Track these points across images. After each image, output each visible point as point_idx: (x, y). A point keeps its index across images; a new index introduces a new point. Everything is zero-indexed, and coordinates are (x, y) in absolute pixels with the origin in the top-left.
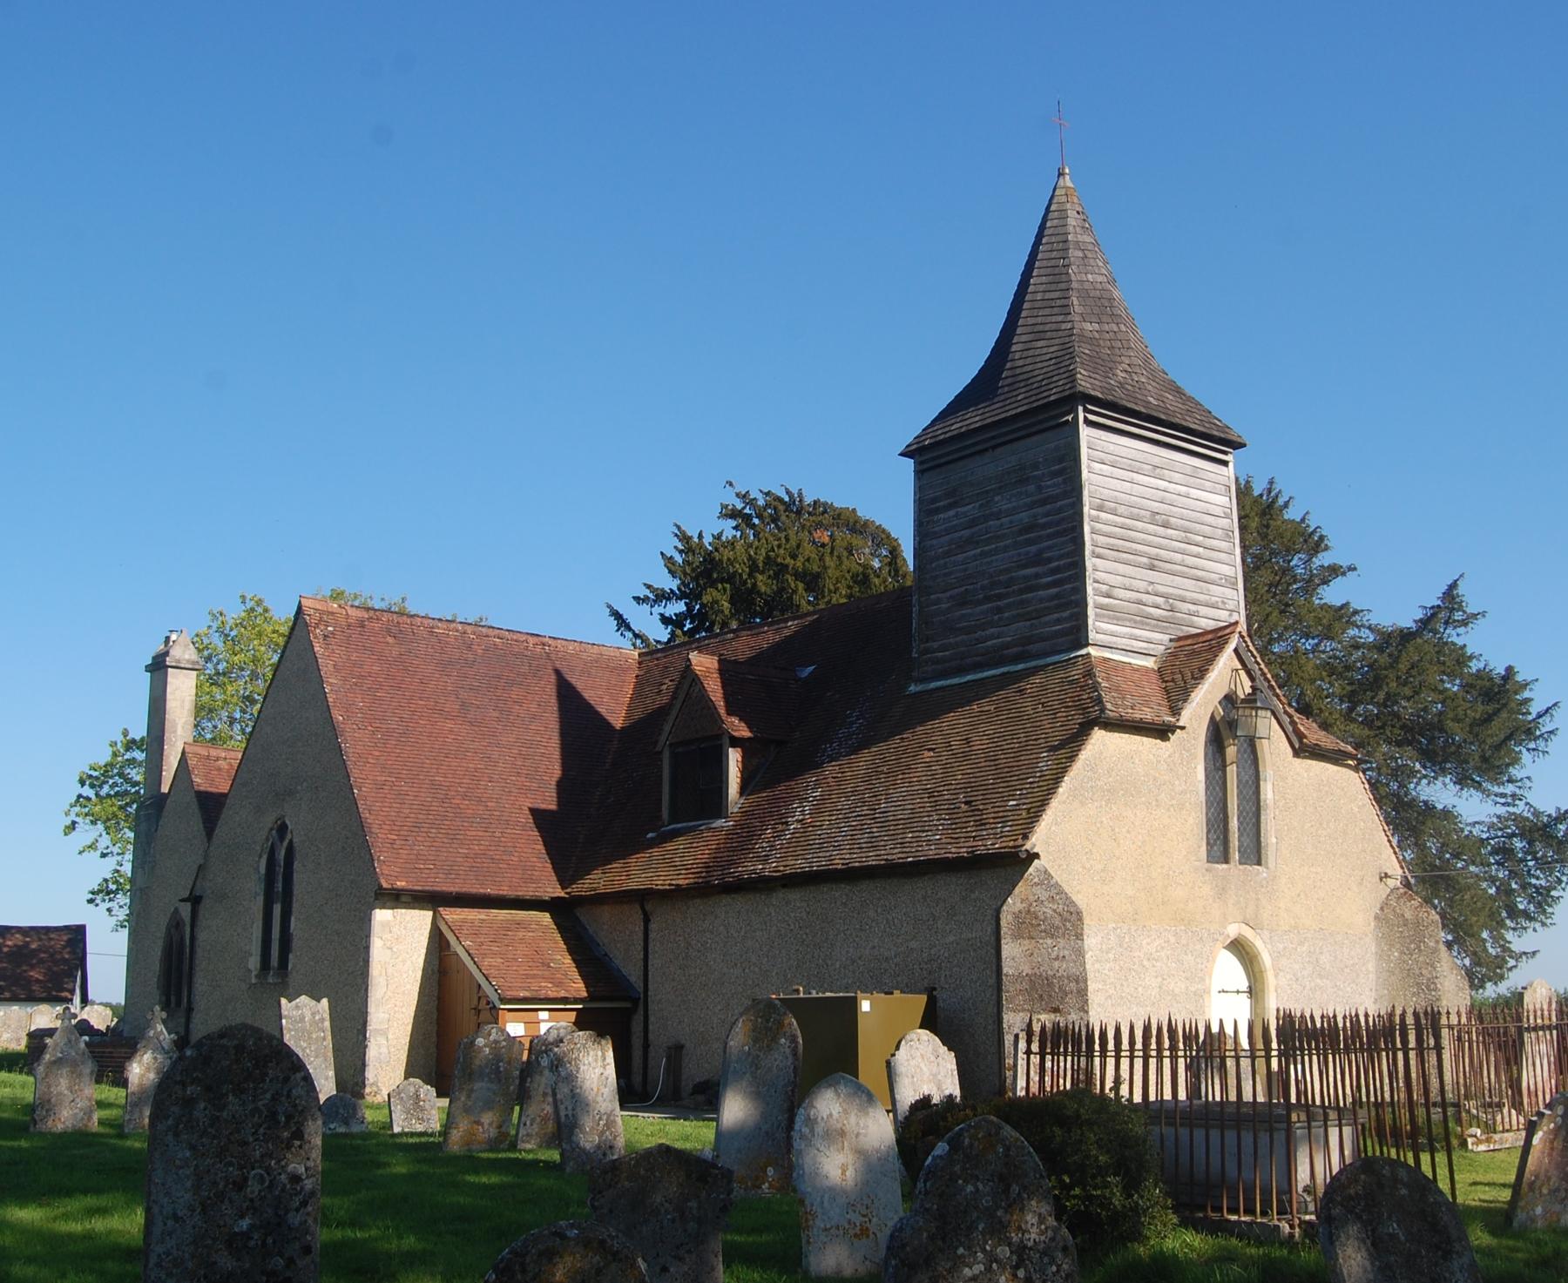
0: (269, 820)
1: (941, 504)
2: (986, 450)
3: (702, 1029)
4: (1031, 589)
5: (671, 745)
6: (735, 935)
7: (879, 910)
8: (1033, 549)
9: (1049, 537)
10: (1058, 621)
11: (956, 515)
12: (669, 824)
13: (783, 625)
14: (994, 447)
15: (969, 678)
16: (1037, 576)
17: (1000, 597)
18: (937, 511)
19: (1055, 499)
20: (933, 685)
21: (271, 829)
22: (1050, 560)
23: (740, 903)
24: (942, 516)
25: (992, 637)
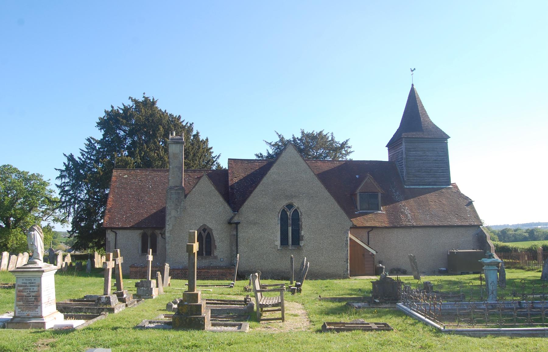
0: (285, 203)
1: (411, 150)
2: (424, 142)
3: (388, 257)
4: (437, 172)
5: (359, 192)
6: (400, 237)
7: (445, 234)
8: (437, 164)
9: (441, 163)
10: (443, 180)
11: (416, 153)
12: (360, 210)
13: (332, 162)
14: (426, 142)
15: (421, 187)
16: (438, 170)
17: (428, 172)
18: (410, 151)
19: (442, 156)
20: (411, 187)
21: (284, 205)
22: (441, 167)
23: (401, 230)
24: (412, 152)
25: (426, 180)
